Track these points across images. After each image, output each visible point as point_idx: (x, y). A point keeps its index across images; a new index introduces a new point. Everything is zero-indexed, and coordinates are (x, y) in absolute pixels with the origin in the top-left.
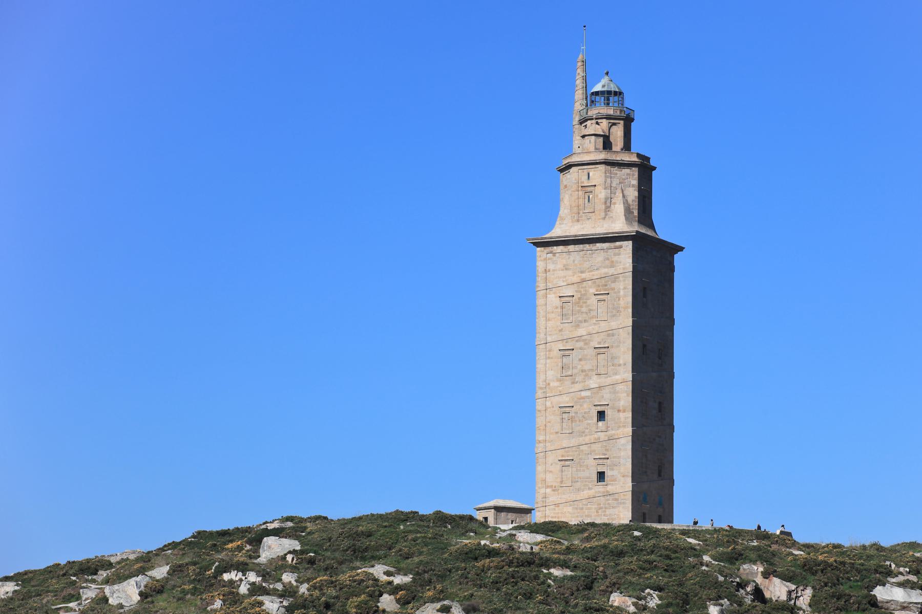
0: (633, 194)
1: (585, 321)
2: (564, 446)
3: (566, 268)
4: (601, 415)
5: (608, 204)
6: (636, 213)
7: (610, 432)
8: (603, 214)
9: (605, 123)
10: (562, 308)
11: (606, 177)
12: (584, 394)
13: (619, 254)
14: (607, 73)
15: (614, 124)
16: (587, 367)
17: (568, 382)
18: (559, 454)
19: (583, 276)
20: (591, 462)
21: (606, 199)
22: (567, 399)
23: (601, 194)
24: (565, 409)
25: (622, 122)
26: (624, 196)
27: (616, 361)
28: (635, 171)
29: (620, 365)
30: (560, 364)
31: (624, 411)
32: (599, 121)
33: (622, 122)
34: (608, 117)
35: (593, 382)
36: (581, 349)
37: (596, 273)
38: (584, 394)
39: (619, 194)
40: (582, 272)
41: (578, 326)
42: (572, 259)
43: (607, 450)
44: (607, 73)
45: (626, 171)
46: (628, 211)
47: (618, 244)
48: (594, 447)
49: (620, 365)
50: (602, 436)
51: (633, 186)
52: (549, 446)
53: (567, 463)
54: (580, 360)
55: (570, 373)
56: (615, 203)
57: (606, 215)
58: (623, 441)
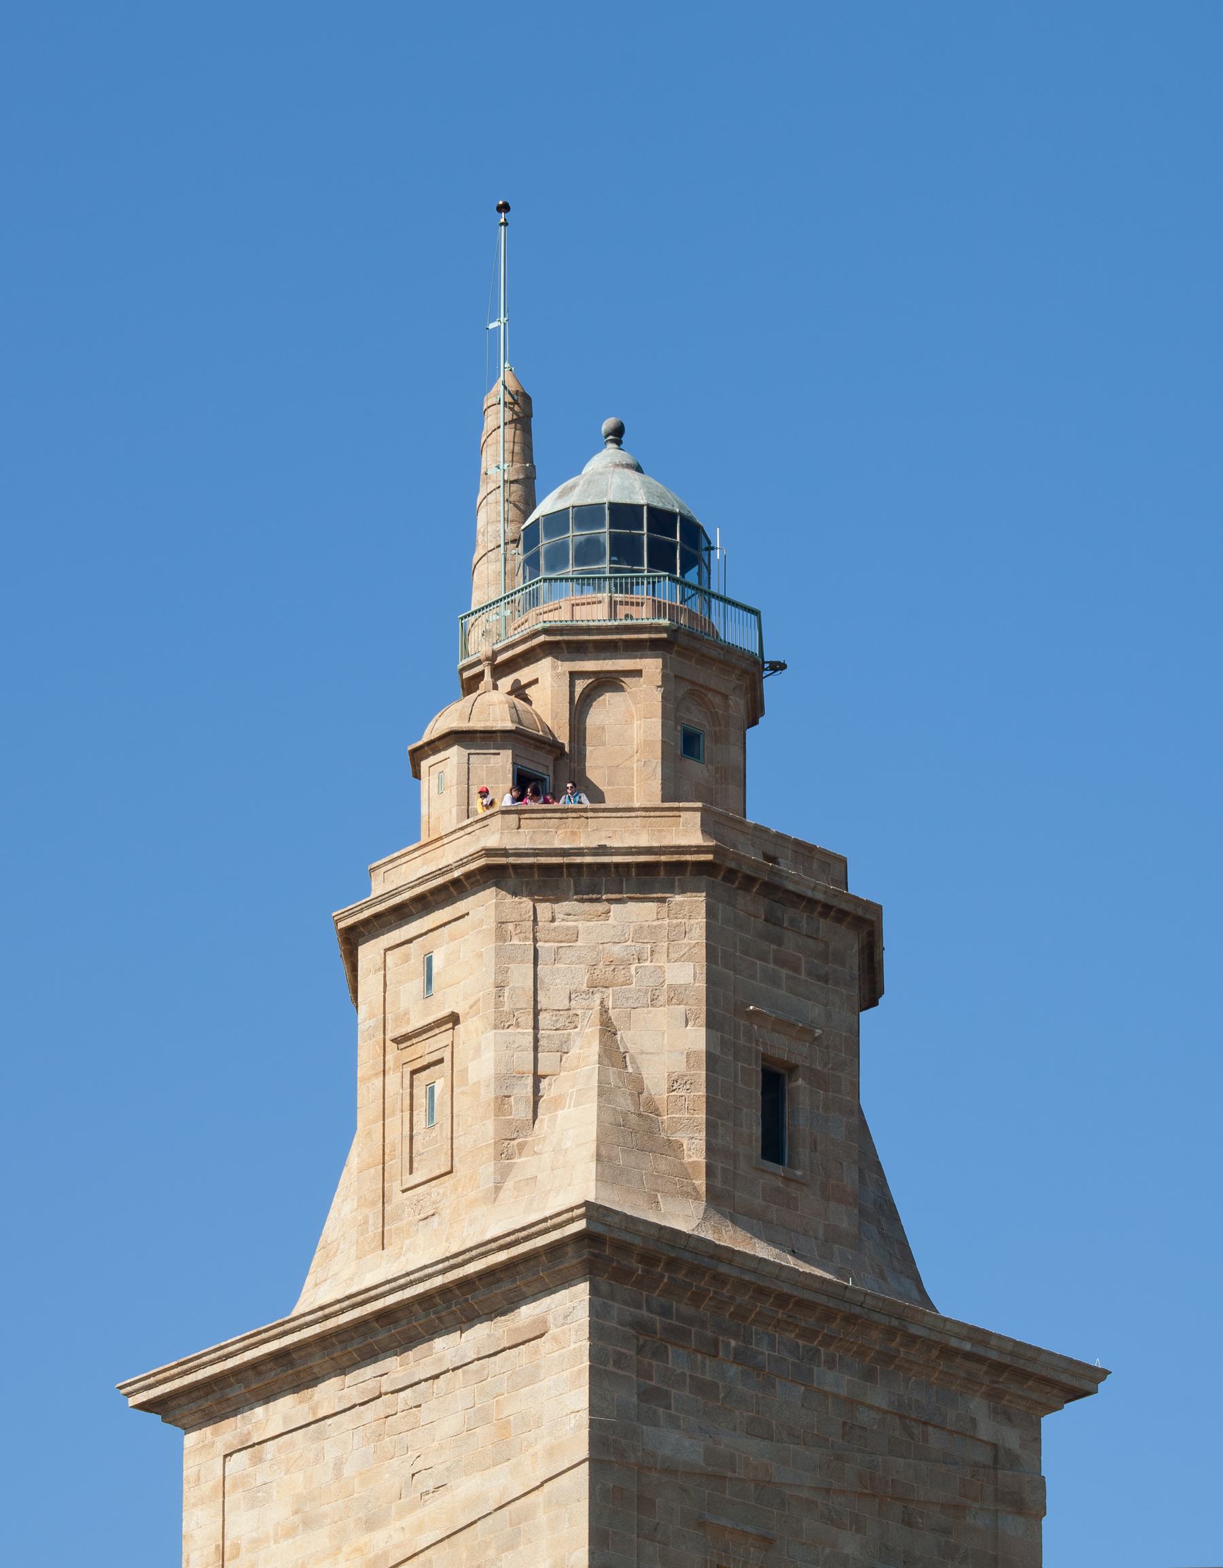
0: (672, 1045)
3: (305, 1519)
5: (522, 1111)
6: (694, 1150)
8: (487, 1171)
9: (548, 683)
11: (503, 960)
13: (533, 1378)
14: (618, 434)
15: (608, 682)
21: (505, 1080)
23: (481, 1054)
25: (652, 666)
26: (612, 1053)
28: (690, 911)
32: (524, 675)
33: (652, 666)
34: (564, 643)
37: (434, 1506)
39: (586, 1046)
40: (371, 1524)
42: (331, 1455)
44: (618, 434)
45: (635, 914)
46: (630, 1129)
47: (527, 1313)
51: (676, 995)
56: (558, 1103)
57: (502, 1175)
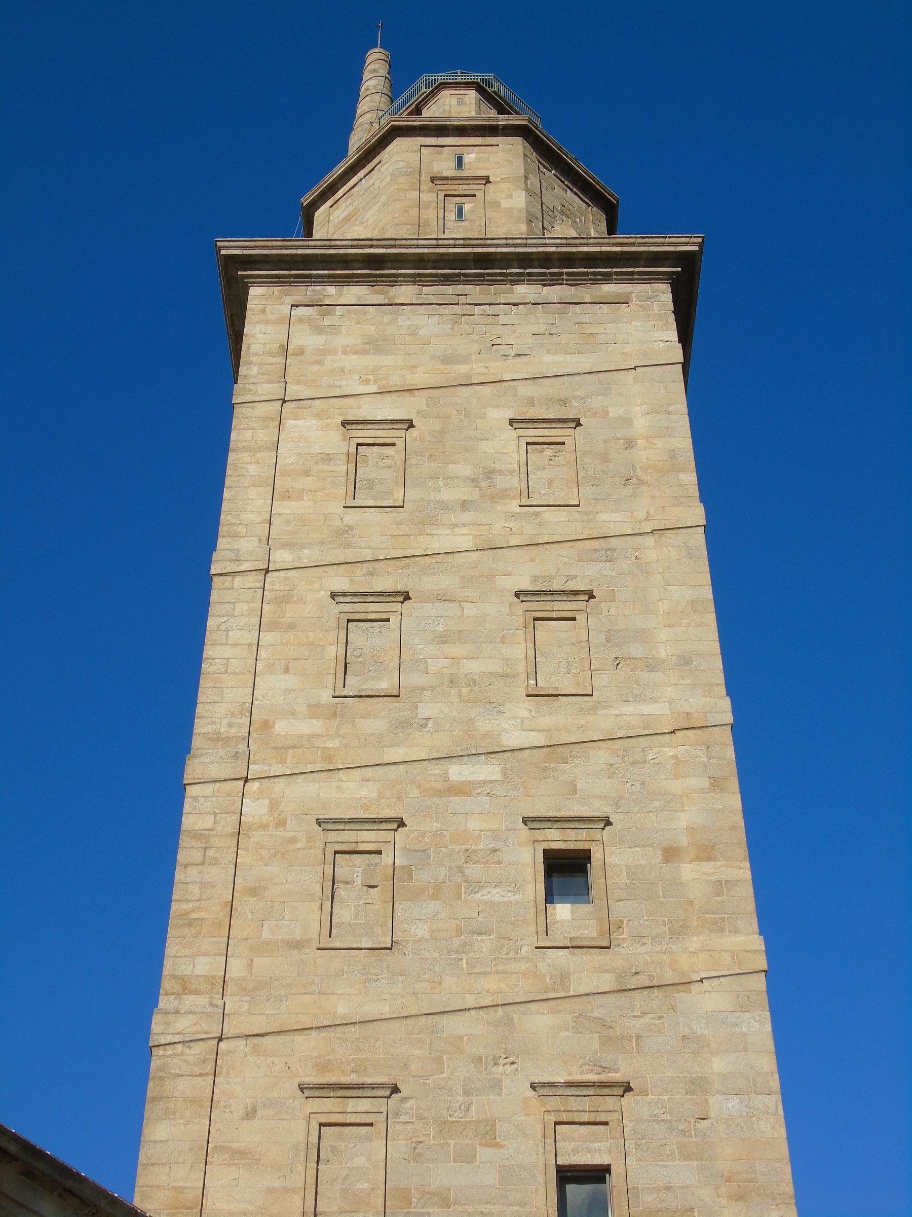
1: (465, 505)
2: (343, 1009)
4: (566, 871)
7: (630, 952)
10: (355, 460)
12: (458, 772)
16: (473, 667)
17: (375, 721)
18: (305, 1056)
19: (462, 369)
20: (513, 1103)
22: (368, 792)
24: (350, 839)
27: (636, 650)
29: (651, 665)
30: (333, 651)
31: (706, 852)
35: (519, 724)
36: (443, 598)
38: (458, 772)
41: (428, 519)
43: (608, 1042)
47: (609, 289)
48: (539, 1022)
49: (651, 665)
50: (588, 973)
52: (244, 1015)
53: (359, 1107)
54: (443, 639)
55: (383, 685)
58: (710, 1000)
